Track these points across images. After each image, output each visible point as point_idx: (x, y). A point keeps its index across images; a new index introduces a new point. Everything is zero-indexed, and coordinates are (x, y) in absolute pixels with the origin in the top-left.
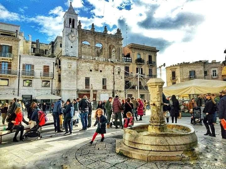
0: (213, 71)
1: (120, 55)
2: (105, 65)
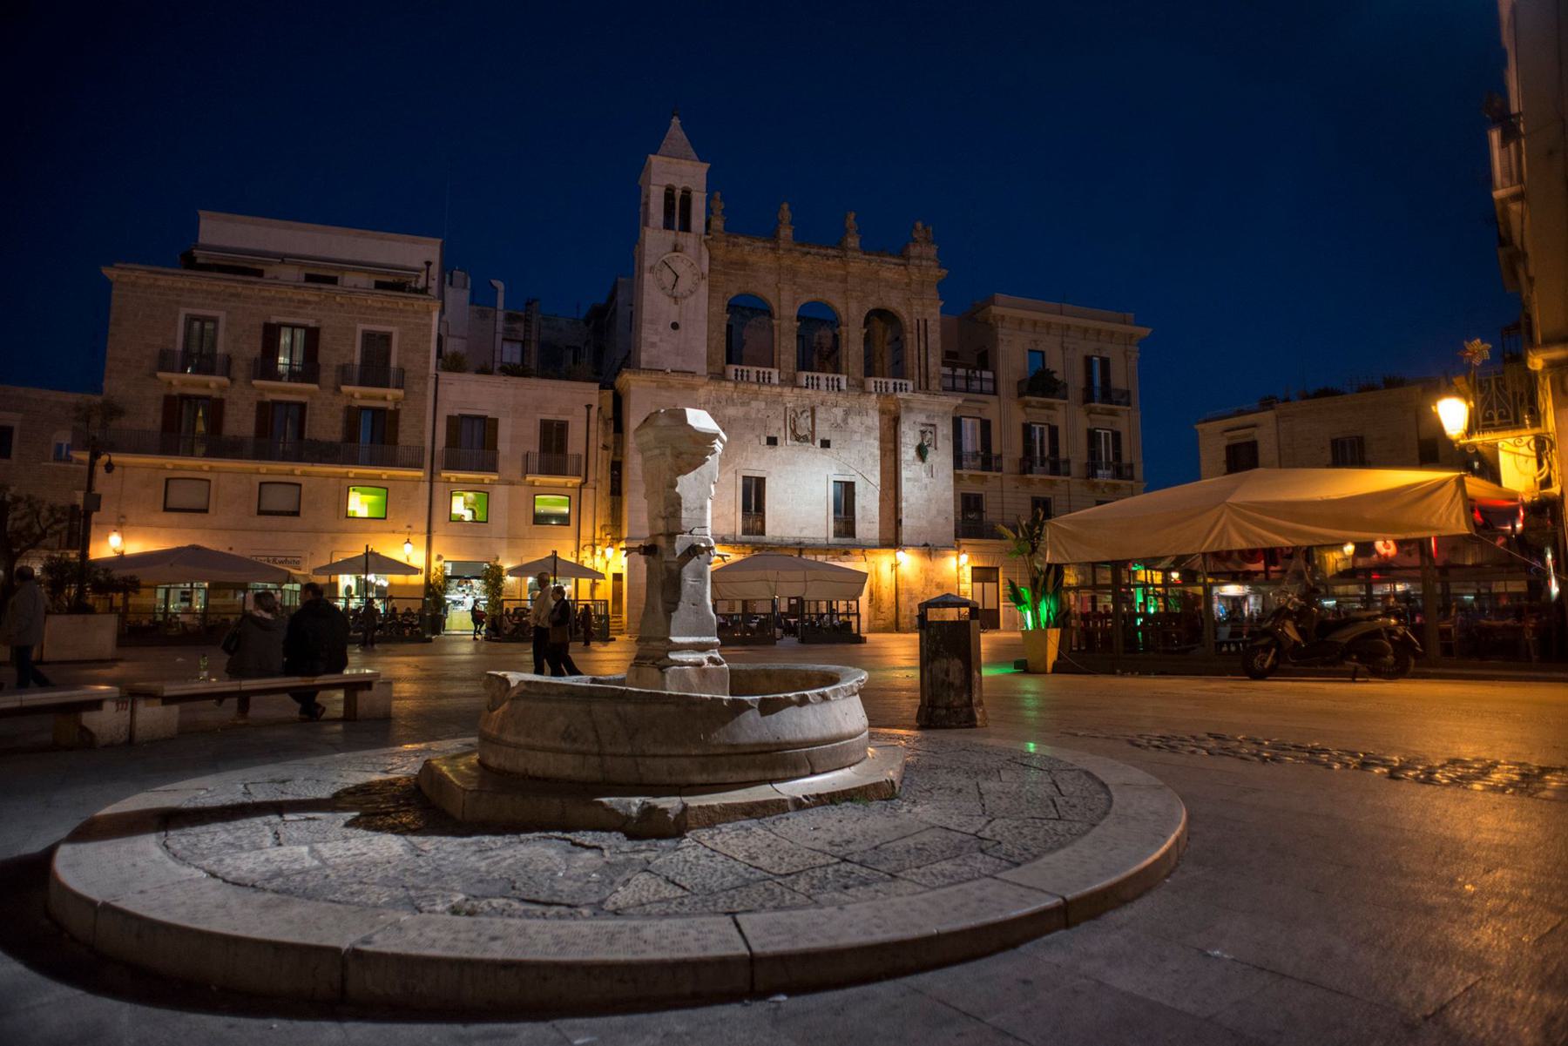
1: (931, 360)
2: (847, 413)
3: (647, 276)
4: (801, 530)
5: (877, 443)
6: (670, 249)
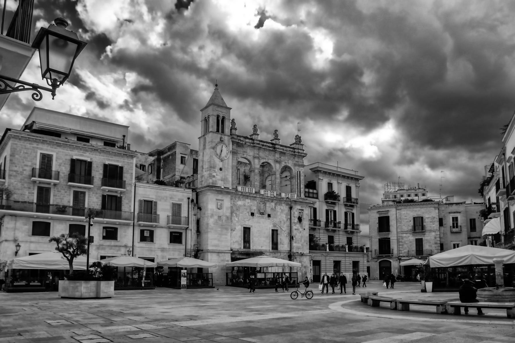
0: (453, 218)
1: (301, 186)
4: (262, 247)
5: (285, 216)
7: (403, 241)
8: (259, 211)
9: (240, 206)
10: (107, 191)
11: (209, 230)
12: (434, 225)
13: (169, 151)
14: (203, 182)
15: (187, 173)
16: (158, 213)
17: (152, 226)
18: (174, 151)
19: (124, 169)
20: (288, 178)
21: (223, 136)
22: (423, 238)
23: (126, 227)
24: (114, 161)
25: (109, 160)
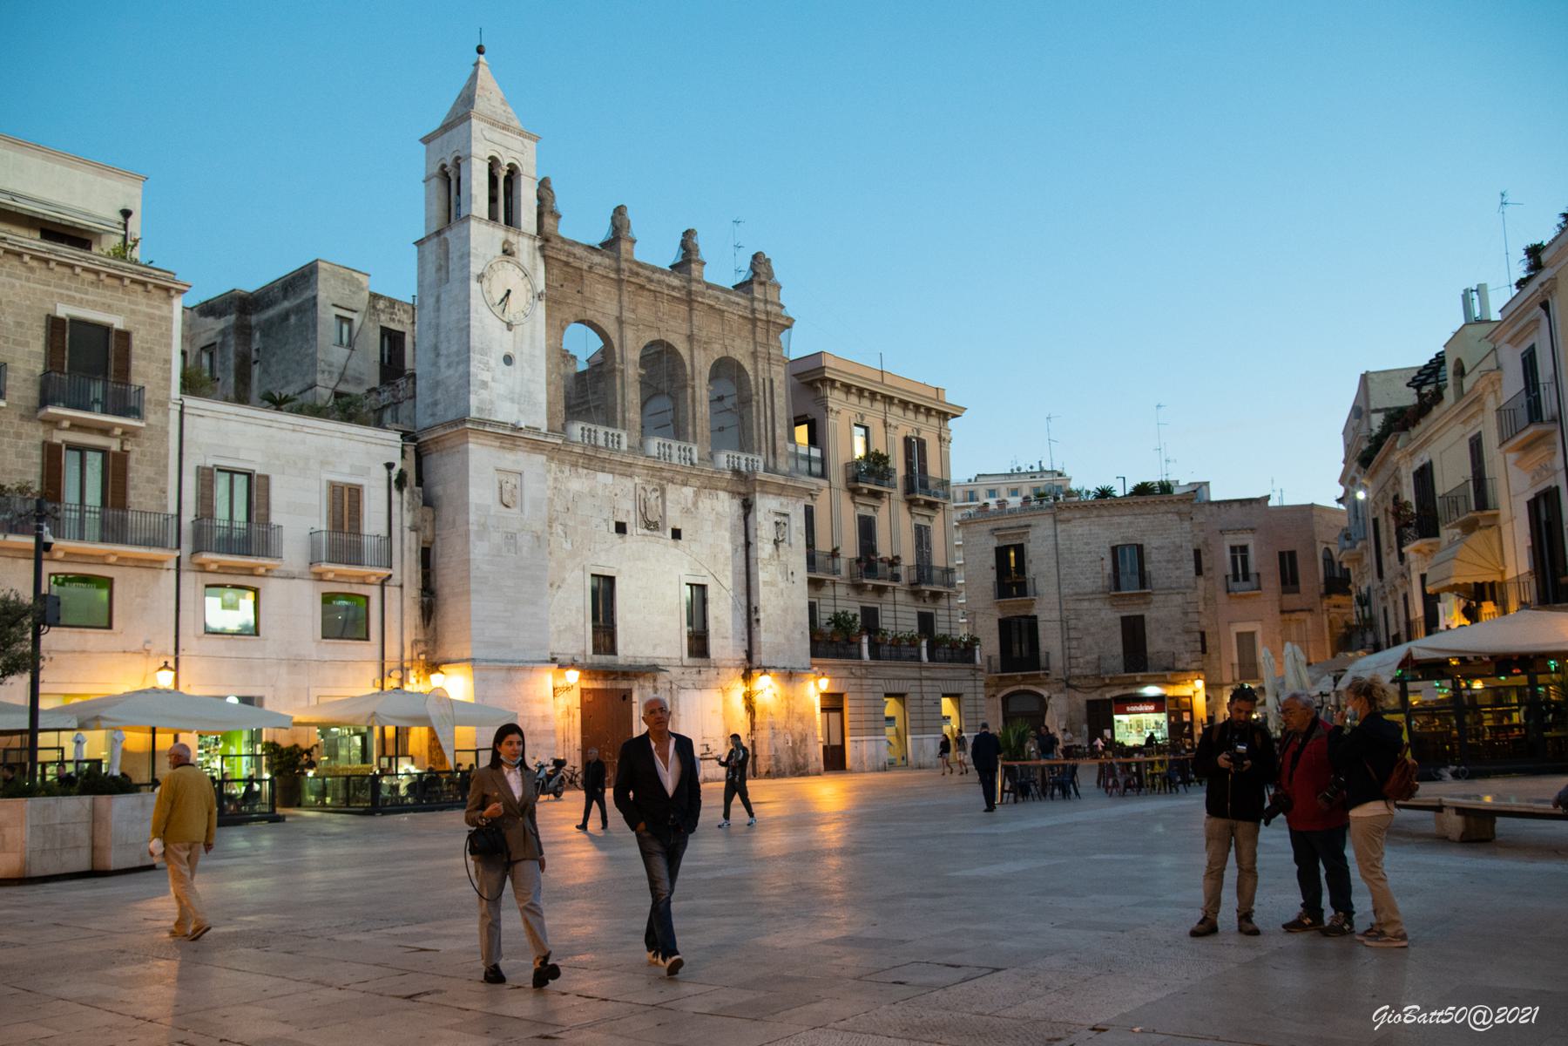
0: (1233, 549)
1: (778, 431)
2: (696, 494)
3: (474, 286)
4: (655, 647)
5: (727, 535)
6: (499, 252)
7: (1081, 625)
8: (644, 515)
9: (577, 498)
10: (66, 424)
11: (473, 586)
12: (1178, 573)
13: (285, 297)
14: (441, 407)
15: (359, 381)
16: (275, 518)
17: (251, 571)
18: (308, 294)
19: (136, 342)
20: (728, 403)
21: (512, 238)
22: (1147, 614)
23: (146, 575)
24: (93, 305)
25: (70, 300)
